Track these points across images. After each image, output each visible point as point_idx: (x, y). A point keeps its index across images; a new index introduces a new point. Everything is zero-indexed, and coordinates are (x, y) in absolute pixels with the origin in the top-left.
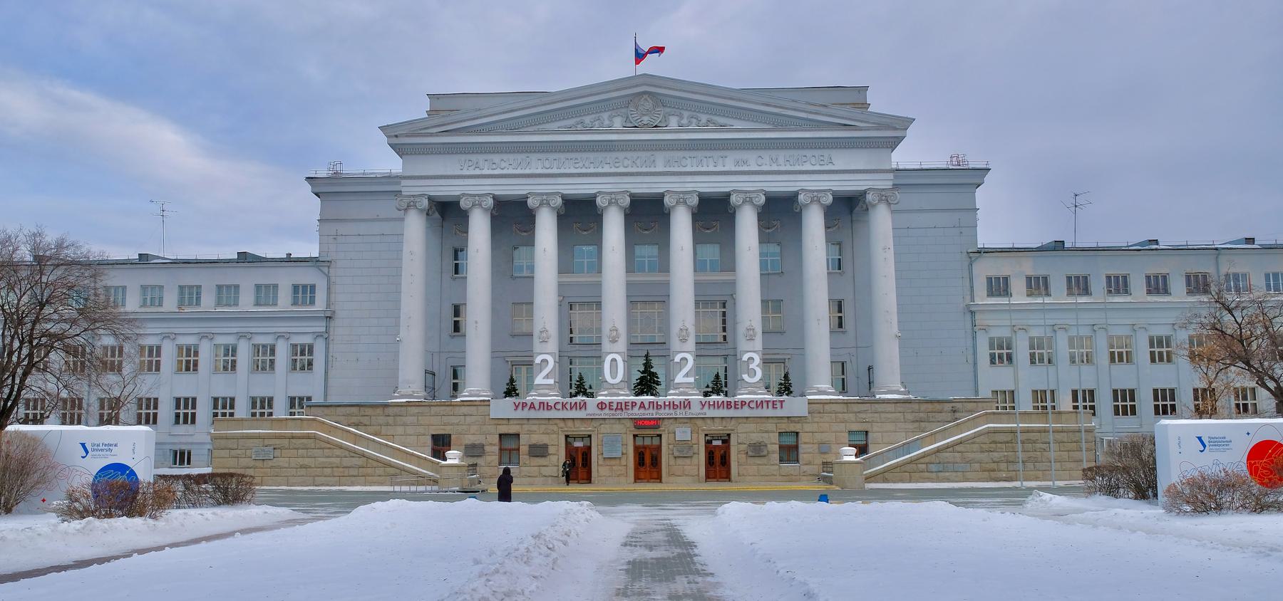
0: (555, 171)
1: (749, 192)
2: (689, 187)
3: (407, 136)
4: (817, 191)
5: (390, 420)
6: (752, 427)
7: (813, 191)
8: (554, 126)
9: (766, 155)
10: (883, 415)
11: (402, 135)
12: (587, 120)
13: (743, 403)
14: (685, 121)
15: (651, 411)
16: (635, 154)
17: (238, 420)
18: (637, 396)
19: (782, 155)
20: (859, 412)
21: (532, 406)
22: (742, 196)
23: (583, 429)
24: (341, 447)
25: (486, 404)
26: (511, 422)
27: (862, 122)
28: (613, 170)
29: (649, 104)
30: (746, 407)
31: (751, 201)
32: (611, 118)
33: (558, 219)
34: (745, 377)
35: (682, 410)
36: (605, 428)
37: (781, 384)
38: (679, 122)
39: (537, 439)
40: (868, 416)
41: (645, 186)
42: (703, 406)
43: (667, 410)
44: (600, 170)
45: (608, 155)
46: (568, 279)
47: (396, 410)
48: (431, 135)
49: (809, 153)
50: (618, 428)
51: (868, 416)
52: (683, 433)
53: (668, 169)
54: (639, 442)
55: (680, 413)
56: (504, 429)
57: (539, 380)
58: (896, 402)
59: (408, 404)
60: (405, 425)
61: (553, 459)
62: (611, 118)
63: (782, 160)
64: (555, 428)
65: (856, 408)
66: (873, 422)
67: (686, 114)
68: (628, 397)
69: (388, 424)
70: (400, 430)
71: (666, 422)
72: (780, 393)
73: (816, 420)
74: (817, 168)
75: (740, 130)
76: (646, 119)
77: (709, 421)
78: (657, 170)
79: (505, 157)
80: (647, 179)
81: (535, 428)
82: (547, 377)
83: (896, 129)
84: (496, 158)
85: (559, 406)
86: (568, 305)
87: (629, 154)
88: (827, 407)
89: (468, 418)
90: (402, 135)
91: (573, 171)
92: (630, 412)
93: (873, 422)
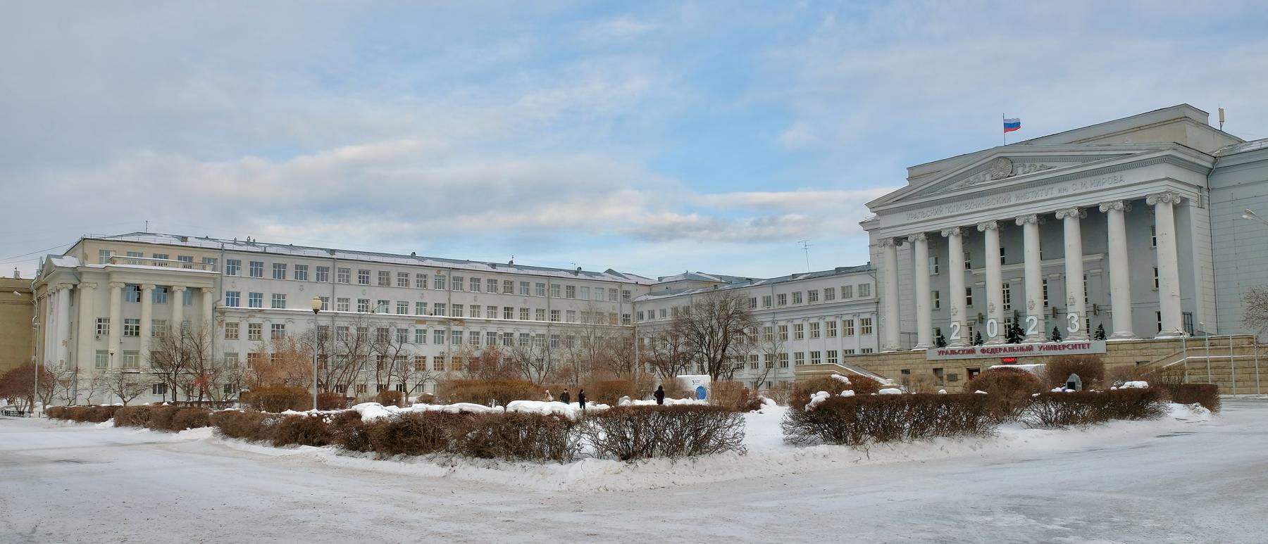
0: (955, 213)
1: (1068, 209)
2: (1031, 211)
4: (1112, 202)
7: (1109, 202)
8: (954, 187)
9: (1078, 182)
10: (1160, 351)
12: (971, 179)
13: (1064, 346)
14: (1027, 170)
15: (1010, 353)
16: (998, 196)
18: (1008, 343)
19: (1088, 180)
21: (947, 353)
22: (1065, 212)
26: (939, 362)
27: (1137, 150)
28: (987, 208)
29: (1003, 163)
30: (1066, 349)
31: (1069, 215)
32: (984, 175)
34: (1069, 329)
35: (1029, 352)
37: (1097, 332)
38: (1023, 170)
41: (1005, 214)
42: (1040, 349)
43: (1020, 352)
44: (980, 209)
45: (983, 199)
46: (1007, 268)
47: (883, 357)
48: (890, 204)
53: (1018, 202)
56: (935, 366)
57: (953, 337)
58: (1169, 341)
59: (889, 354)
60: (888, 365)
61: (961, 383)
62: (984, 175)
63: (1089, 183)
64: (960, 364)
65: (1139, 346)
66: (1152, 355)
67: (1027, 164)
68: (1002, 343)
71: (1020, 359)
73: (1113, 355)
74: (1113, 185)
75: (1063, 168)
77: (1045, 358)
78: (1012, 203)
79: (929, 209)
81: (950, 365)
82: (957, 335)
83: (1161, 151)
84: (925, 210)
85: (961, 352)
87: (995, 196)
88: (1120, 346)
89: (917, 360)
91: (967, 211)
93: (1152, 355)
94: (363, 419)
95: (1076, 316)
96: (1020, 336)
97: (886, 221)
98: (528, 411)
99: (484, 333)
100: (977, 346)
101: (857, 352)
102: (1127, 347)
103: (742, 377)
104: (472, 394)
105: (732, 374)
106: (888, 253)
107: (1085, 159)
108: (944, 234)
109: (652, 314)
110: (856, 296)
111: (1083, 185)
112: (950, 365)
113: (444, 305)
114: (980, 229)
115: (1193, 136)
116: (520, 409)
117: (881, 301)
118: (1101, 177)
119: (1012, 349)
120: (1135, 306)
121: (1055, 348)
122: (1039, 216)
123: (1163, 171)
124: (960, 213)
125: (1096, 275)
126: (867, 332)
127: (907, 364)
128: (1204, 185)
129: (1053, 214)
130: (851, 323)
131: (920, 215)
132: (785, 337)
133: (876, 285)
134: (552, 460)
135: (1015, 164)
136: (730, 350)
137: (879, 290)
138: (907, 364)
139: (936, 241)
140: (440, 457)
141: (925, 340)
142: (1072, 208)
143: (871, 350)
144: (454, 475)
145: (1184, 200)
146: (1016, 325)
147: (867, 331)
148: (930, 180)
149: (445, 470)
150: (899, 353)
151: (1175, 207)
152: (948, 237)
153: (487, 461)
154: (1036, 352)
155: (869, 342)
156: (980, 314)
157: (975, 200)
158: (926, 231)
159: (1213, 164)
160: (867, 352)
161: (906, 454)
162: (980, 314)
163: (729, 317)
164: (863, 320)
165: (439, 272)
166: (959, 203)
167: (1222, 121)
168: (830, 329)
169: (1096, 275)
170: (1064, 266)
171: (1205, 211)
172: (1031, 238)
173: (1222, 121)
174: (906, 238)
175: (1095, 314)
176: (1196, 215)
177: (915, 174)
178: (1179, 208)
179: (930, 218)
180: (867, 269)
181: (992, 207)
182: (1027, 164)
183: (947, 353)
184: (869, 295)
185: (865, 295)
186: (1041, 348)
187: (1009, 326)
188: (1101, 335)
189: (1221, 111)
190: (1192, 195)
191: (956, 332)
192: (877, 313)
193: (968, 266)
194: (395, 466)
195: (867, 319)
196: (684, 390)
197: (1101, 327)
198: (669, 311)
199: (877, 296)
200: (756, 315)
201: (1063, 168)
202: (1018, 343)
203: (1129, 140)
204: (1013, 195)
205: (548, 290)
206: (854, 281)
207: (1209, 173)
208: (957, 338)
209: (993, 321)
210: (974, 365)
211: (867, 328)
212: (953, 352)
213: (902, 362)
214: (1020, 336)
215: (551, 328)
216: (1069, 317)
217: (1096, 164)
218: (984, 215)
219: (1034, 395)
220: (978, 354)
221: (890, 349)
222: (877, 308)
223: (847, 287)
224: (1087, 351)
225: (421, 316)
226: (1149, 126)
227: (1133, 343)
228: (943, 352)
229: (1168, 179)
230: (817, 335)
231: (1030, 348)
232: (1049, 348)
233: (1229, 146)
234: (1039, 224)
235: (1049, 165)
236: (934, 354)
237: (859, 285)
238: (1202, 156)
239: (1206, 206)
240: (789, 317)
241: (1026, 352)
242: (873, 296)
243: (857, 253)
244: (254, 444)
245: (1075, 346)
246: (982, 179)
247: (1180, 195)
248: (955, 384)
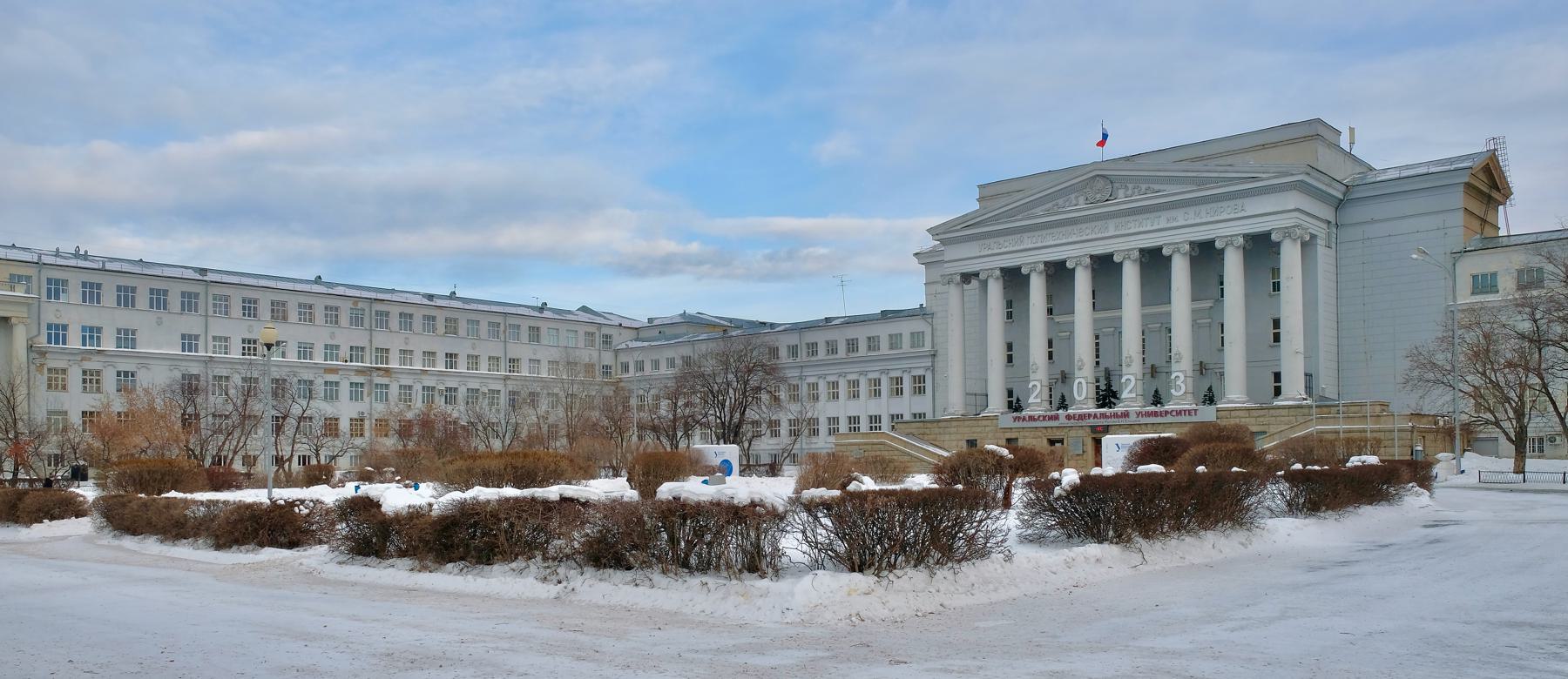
0: (1039, 245)
1: (1177, 243)
3: (944, 233)
4: (1230, 236)
5: (941, 430)
8: (1039, 211)
9: (1191, 210)
10: (1278, 418)
11: (941, 234)
12: (1060, 202)
13: (1167, 412)
14: (1130, 192)
15: (1102, 420)
16: (1093, 224)
17: (863, 434)
18: (1099, 408)
19: (1203, 208)
20: (1258, 417)
21: (1024, 419)
24: (897, 449)
26: (1014, 430)
27: (1263, 173)
28: (1079, 239)
29: (1100, 184)
31: (1179, 251)
32: (1077, 197)
33: (1047, 281)
34: (1173, 391)
35: (1123, 419)
36: (1073, 433)
37: (1205, 395)
38: (1125, 194)
40: (1265, 420)
44: (1070, 240)
47: (944, 424)
48: (957, 231)
49: (1225, 204)
50: (1081, 432)
51: (1265, 420)
55: (1122, 421)
56: (1009, 435)
58: (1290, 407)
63: (1204, 213)
64: (1040, 434)
65: (1255, 413)
67: (1130, 186)
68: (1090, 408)
69: (940, 434)
70: (947, 437)
71: (1113, 428)
72: (1204, 403)
74: (1232, 216)
75: (1174, 192)
77: (1143, 427)
80: (1102, 242)
81: (1027, 434)
83: (1292, 175)
84: (1001, 240)
85: (1041, 419)
90: (941, 234)
91: (1053, 243)
92: (1088, 421)
93: (1269, 424)
94: (383, 509)
95: (1182, 378)
96: (1112, 400)
97: (952, 253)
98: (703, 498)
99: (418, 387)
100: (1061, 411)
101: (907, 417)
102: (1241, 414)
103: (817, 446)
104: (483, 470)
105: (750, 444)
106: (953, 292)
107: (1202, 182)
108: (1024, 271)
109: (640, 366)
111: (1197, 215)
112: (1027, 434)
113: (363, 349)
114: (1069, 265)
115: (1326, 159)
116: (683, 496)
117: (940, 352)
118: (1220, 204)
119: (1103, 416)
120: (1252, 363)
121: (1155, 414)
122: (1142, 251)
123: (1293, 200)
124: (1044, 244)
125: (1209, 326)
126: (920, 393)
127: (974, 433)
128: (1332, 220)
129: (1159, 249)
130: (899, 380)
131: (994, 246)
132: (816, 398)
133: (932, 334)
134: (746, 573)
135: (1116, 185)
136: (751, 414)
137: (935, 338)
138: (974, 433)
139: (1014, 279)
140: (536, 565)
141: (997, 403)
142: (1180, 243)
143: (924, 414)
144: (573, 597)
145: (1313, 237)
146: (1109, 385)
147: (920, 391)
148: (1010, 201)
149: (552, 589)
150: (963, 419)
151: (1304, 245)
152: (1029, 275)
153: (629, 575)
154: (1132, 419)
155: (923, 404)
156: (1063, 372)
157: (1063, 229)
158: (1002, 266)
159: (1345, 194)
160: (919, 417)
161: (1181, 555)
162: (1063, 372)
163: (750, 371)
164: (915, 377)
165: (355, 303)
166: (1044, 232)
167: (1352, 143)
168: (873, 388)
169: (1209, 326)
170: (1169, 314)
171: (1332, 252)
172: (1131, 277)
173: (1352, 143)
174: (976, 275)
175: (1202, 373)
176: (1323, 254)
177: (988, 193)
178: (1307, 246)
179: (1007, 249)
180: (921, 313)
181: (1084, 238)
182: (1130, 186)
183: (1024, 419)
184: (923, 345)
185: (918, 346)
186: (1139, 414)
187: (1098, 387)
188: (1210, 399)
189: (1352, 130)
190: (1319, 229)
191: (1035, 394)
192: (933, 369)
193: (1050, 311)
194: (449, 580)
195: (920, 377)
196: (707, 463)
197: (1210, 389)
198: (678, 362)
199: (933, 347)
200: (784, 368)
201: (1174, 192)
202: (1110, 407)
203: (1251, 162)
204: (1112, 224)
205: (504, 332)
206: (905, 328)
207: (1339, 205)
208: (1036, 403)
209: (1180, 374)
210: (1057, 435)
211: (920, 387)
212: (1032, 418)
213: (967, 430)
214: (1112, 400)
215: (508, 382)
216: (1173, 377)
217: (1213, 188)
218: (1075, 249)
219: (1279, 473)
220: (1063, 421)
221: (954, 414)
222: (933, 362)
223: (896, 335)
224: (1194, 419)
225: (357, 364)
226: (1275, 145)
227: (1248, 409)
228: (1019, 418)
229: (1297, 210)
230: (856, 396)
231: (1126, 415)
232: (1149, 414)
233: (1359, 173)
234: (1141, 261)
235: (1157, 187)
236: (1008, 420)
237: (912, 334)
238: (1334, 183)
239: (1334, 246)
240: (862, 369)
241: (1120, 420)
242: (928, 347)
243: (910, 292)
244: (175, 545)
245: (1179, 413)
246: (1074, 202)
247: (1310, 230)
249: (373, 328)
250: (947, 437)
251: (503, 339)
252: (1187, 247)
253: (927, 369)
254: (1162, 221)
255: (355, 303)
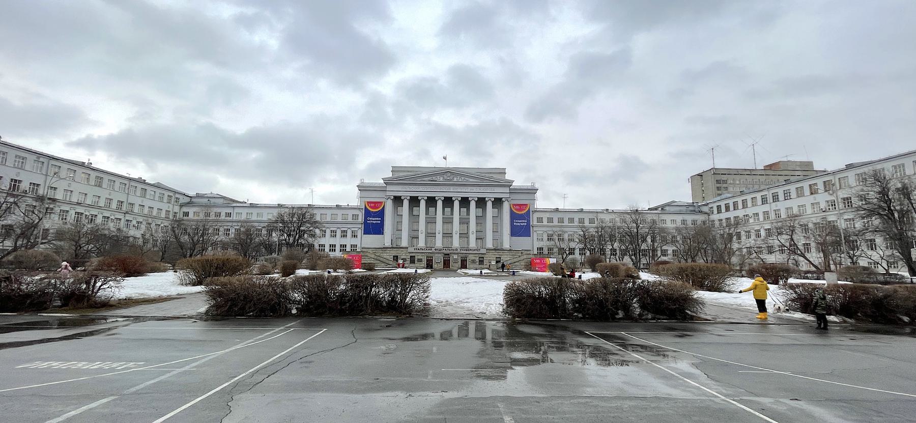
6: (472, 255)
12: (434, 178)
23: (431, 255)
25: (407, 248)
29: (449, 174)
36: (436, 255)
39: (419, 257)
50: (439, 255)
52: (455, 257)
54: (445, 259)
63: (482, 189)
67: (458, 177)
76: (448, 178)
84: (411, 187)
86: (427, 223)
97: (389, 188)
99: (72, 213)
110: (350, 219)
113: (38, 185)
131: (408, 188)
165: (38, 158)
184: (358, 219)
205: (128, 189)
215: (126, 215)
235: (467, 179)
248: (421, 263)
249: (49, 174)
250: (385, 254)
251: (127, 192)
252: (409, 198)
253: (360, 228)
254: (469, 189)
255: (38, 158)
